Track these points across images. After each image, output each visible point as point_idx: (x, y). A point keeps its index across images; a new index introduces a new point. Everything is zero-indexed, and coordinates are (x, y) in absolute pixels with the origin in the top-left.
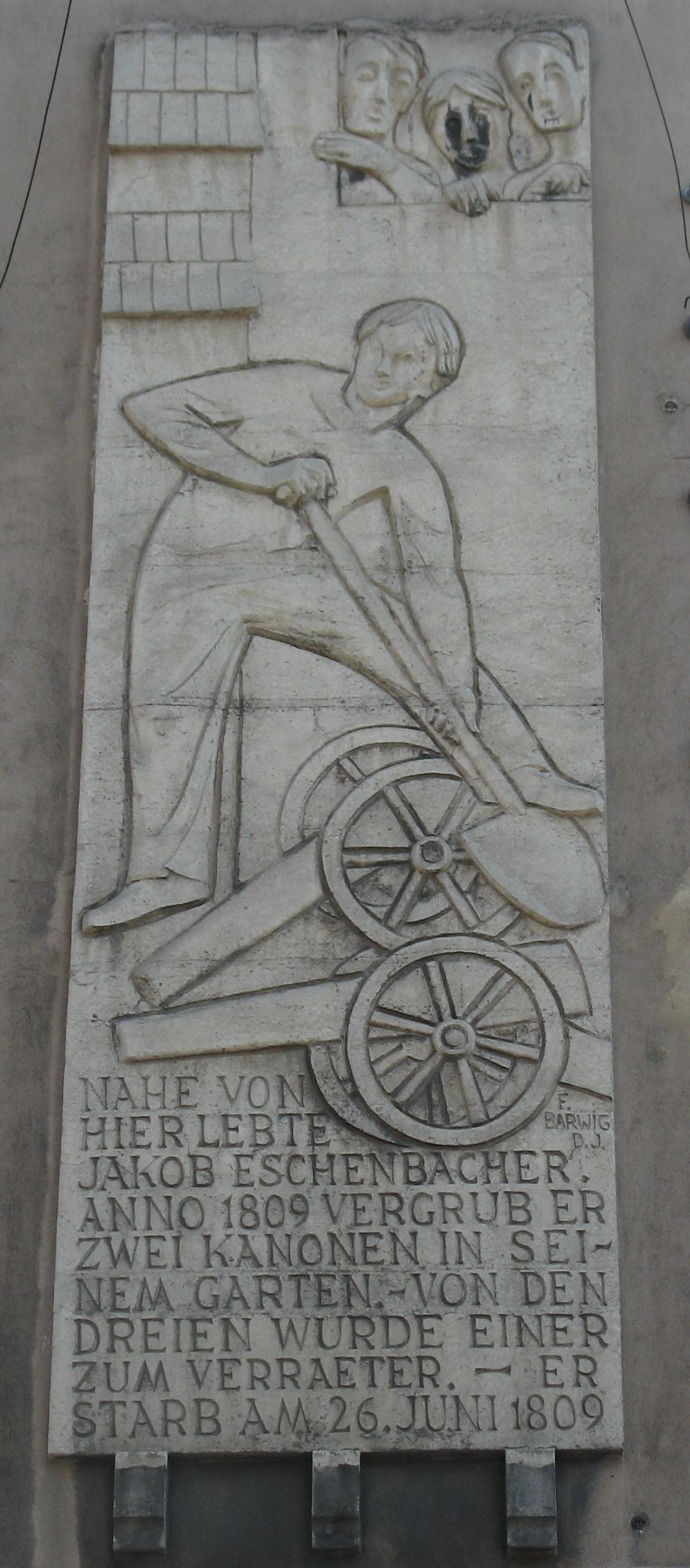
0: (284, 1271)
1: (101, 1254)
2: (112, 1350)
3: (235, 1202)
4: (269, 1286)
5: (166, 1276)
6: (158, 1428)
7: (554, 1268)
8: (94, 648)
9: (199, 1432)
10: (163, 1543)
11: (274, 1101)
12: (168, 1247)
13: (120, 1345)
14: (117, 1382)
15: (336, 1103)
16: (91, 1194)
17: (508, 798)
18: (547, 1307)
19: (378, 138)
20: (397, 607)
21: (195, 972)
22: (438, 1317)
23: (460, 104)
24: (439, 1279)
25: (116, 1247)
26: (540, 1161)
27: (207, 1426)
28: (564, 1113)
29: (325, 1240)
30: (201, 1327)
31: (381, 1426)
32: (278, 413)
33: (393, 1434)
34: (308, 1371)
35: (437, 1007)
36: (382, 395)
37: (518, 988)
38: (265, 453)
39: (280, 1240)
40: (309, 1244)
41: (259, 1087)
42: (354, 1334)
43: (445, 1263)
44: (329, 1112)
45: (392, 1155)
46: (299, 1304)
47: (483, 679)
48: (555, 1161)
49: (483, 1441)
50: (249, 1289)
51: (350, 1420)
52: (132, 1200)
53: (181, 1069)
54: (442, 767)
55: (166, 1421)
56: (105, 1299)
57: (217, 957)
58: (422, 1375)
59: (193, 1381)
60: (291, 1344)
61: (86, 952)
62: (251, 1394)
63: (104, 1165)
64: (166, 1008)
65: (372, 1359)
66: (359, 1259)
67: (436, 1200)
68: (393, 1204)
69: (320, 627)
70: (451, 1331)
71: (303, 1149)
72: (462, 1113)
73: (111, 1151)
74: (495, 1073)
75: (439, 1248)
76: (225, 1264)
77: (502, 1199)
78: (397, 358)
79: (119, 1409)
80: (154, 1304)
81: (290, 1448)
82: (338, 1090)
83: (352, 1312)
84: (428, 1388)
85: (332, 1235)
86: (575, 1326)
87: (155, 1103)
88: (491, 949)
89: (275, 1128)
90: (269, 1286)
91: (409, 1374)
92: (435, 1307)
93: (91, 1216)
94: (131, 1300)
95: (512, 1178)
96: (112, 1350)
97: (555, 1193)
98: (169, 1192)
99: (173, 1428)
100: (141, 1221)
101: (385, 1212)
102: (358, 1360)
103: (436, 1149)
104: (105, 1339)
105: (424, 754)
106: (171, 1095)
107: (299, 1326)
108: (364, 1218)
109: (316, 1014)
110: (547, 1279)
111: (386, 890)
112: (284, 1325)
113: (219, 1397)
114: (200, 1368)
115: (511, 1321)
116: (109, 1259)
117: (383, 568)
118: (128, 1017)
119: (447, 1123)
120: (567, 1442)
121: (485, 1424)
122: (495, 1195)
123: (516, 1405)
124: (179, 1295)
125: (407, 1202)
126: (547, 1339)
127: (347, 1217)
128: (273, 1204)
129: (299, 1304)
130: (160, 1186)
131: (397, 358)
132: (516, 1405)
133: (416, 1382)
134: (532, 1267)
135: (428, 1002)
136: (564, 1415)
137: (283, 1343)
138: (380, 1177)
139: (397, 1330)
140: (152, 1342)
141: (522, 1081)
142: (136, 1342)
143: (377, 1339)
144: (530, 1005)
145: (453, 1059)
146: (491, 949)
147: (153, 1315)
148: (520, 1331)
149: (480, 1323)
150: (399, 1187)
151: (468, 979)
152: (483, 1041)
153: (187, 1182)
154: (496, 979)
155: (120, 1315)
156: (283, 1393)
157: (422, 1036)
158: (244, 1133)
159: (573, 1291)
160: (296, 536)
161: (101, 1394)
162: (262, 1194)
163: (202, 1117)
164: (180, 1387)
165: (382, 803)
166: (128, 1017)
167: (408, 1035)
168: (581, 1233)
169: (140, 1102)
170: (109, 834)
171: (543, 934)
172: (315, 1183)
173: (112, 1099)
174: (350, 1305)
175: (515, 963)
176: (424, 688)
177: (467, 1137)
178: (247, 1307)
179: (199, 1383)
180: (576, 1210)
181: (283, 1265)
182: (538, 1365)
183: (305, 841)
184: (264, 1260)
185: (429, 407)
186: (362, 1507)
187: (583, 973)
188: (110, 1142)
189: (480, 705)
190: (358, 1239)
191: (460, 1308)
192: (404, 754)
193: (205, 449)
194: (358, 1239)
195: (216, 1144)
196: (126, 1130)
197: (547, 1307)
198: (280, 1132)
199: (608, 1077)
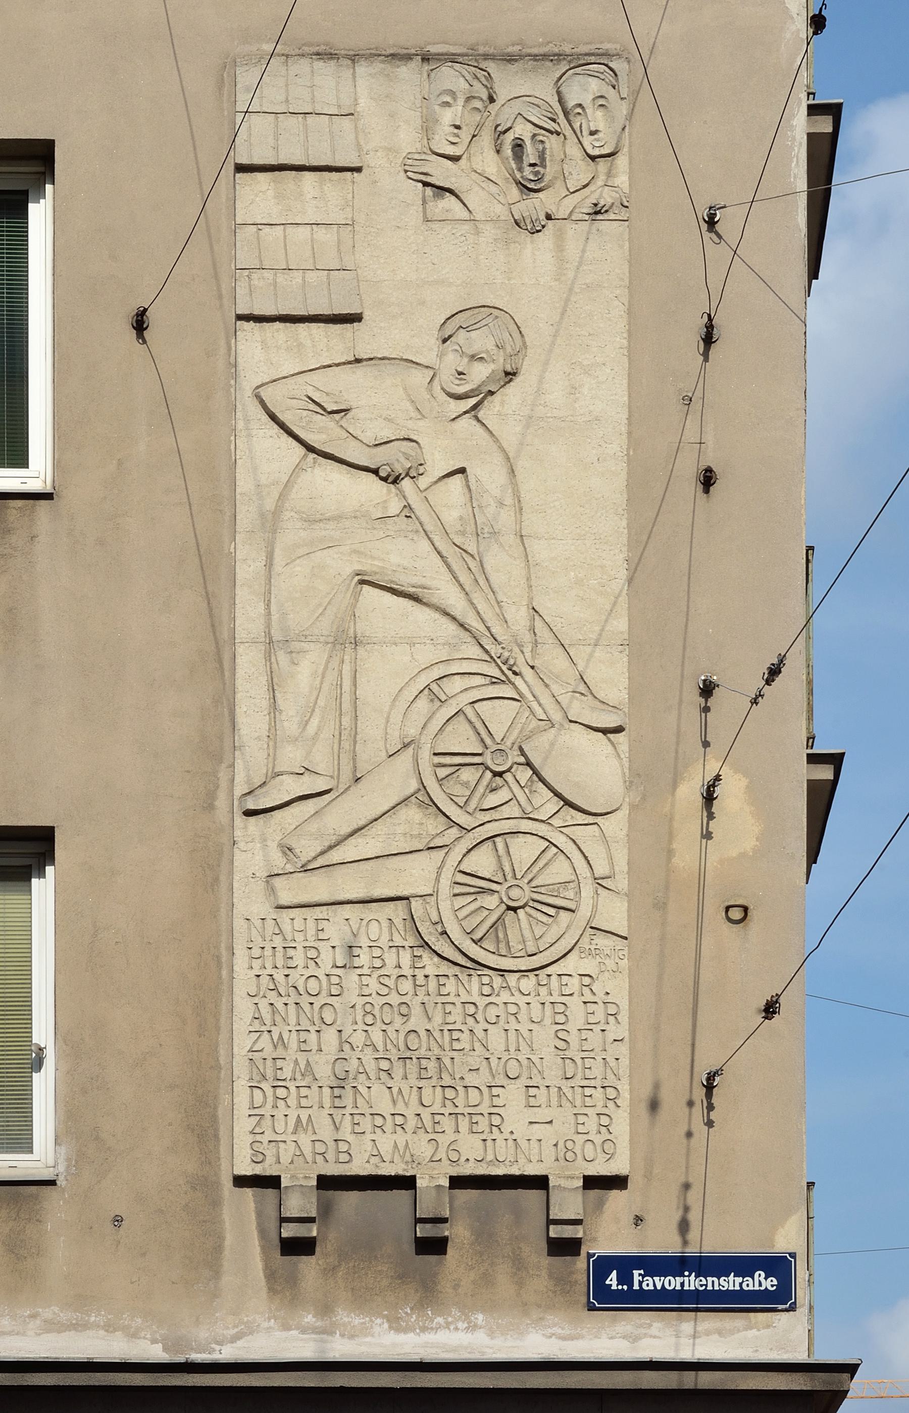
0: (394, 1055)
1: (265, 1042)
2: (275, 1106)
4: (385, 1065)
5: (314, 1058)
6: (309, 1159)
8: (241, 593)
9: (337, 1162)
12: (313, 1036)
13: (281, 1103)
16: (256, 1000)
17: (557, 716)
18: (578, 1081)
19: (455, 159)
20: (472, 564)
21: (327, 844)
23: (523, 130)
24: (503, 1060)
25: (276, 1037)
26: (576, 981)
27: (344, 1157)
29: (423, 1033)
31: (463, 1159)
32: (378, 407)
33: (472, 1163)
34: (412, 1122)
36: (461, 390)
37: (562, 857)
38: (369, 437)
39: (392, 1034)
40: (413, 1035)
47: (538, 623)
48: (587, 981)
49: (532, 1170)
50: (371, 1066)
53: (319, 912)
54: (509, 692)
56: (269, 1073)
57: (342, 833)
59: (332, 1127)
60: (400, 1104)
61: (245, 828)
62: (373, 1137)
63: (265, 980)
64: (305, 869)
66: (447, 1047)
67: (502, 1006)
68: (471, 1009)
69: (415, 580)
70: (513, 1095)
73: (269, 971)
74: (545, 919)
75: (503, 1041)
77: (548, 1006)
78: (473, 358)
79: (282, 1145)
81: (401, 1173)
82: (432, 929)
86: (598, 1094)
87: (299, 937)
88: (542, 829)
89: (386, 956)
90: (385, 1065)
93: (256, 1016)
94: (287, 1073)
95: (556, 993)
96: (275, 1106)
97: (585, 1003)
98: (312, 1000)
99: (319, 1159)
100: (292, 1020)
102: (447, 1115)
103: (502, 972)
104: (270, 1099)
105: (495, 681)
106: (311, 932)
107: (406, 1092)
108: (450, 1019)
109: (415, 875)
110: (579, 1062)
111: (466, 784)
113: (350, 1138)
115: (554, 1090)
116: (271, 1045)
117: (463, 533)
121: (535, 1158)
125: (481, 1008)
126: (578, 1103)
127: (438, 1019)
130: (305, 996)
131: (473, 358)
133: (487, 1130)
134: (568, 1054)
136: (590, 1155)
137: (394, 1102)
138: (462, 991)
140: (304, 1102)
141: (564, 925)
143: (460, 1101)
144: (571, 871)
145: (515, 909)
146: (542, 829)
149: (532, 1091)
150: (475, 998)
151: (524, 851)
152: (535, 896)
155: (280, 1083)
156: (395, 1136)
159: (597, 1070)
160: (395, 506)
161: (269, 1135)
162: (378, 1001)
163: (333, 947)
164: (326, 1132)
165: (461, 718)
167: (483, 891)
169: (289, 938)
170: (259, 738)
171: (580, 818)
175: (560, 840)
176: (493, 631)
179: (337, 1129)
180: (600, 1016)
181: (394, 1051)
182: (572, 1119)
183: (406, 746)
184: (380, 1047)
185: (497, 398)
187: (609, 845)
188: (269, 965)
189: (536, 643)
190: (446, 1033)
191: (517, 1081)
192: (479, 680)
193: (320, 431)
194: (446, 1033)
195: (344, 967)
197: (578, 1081)
198: (390, 958)
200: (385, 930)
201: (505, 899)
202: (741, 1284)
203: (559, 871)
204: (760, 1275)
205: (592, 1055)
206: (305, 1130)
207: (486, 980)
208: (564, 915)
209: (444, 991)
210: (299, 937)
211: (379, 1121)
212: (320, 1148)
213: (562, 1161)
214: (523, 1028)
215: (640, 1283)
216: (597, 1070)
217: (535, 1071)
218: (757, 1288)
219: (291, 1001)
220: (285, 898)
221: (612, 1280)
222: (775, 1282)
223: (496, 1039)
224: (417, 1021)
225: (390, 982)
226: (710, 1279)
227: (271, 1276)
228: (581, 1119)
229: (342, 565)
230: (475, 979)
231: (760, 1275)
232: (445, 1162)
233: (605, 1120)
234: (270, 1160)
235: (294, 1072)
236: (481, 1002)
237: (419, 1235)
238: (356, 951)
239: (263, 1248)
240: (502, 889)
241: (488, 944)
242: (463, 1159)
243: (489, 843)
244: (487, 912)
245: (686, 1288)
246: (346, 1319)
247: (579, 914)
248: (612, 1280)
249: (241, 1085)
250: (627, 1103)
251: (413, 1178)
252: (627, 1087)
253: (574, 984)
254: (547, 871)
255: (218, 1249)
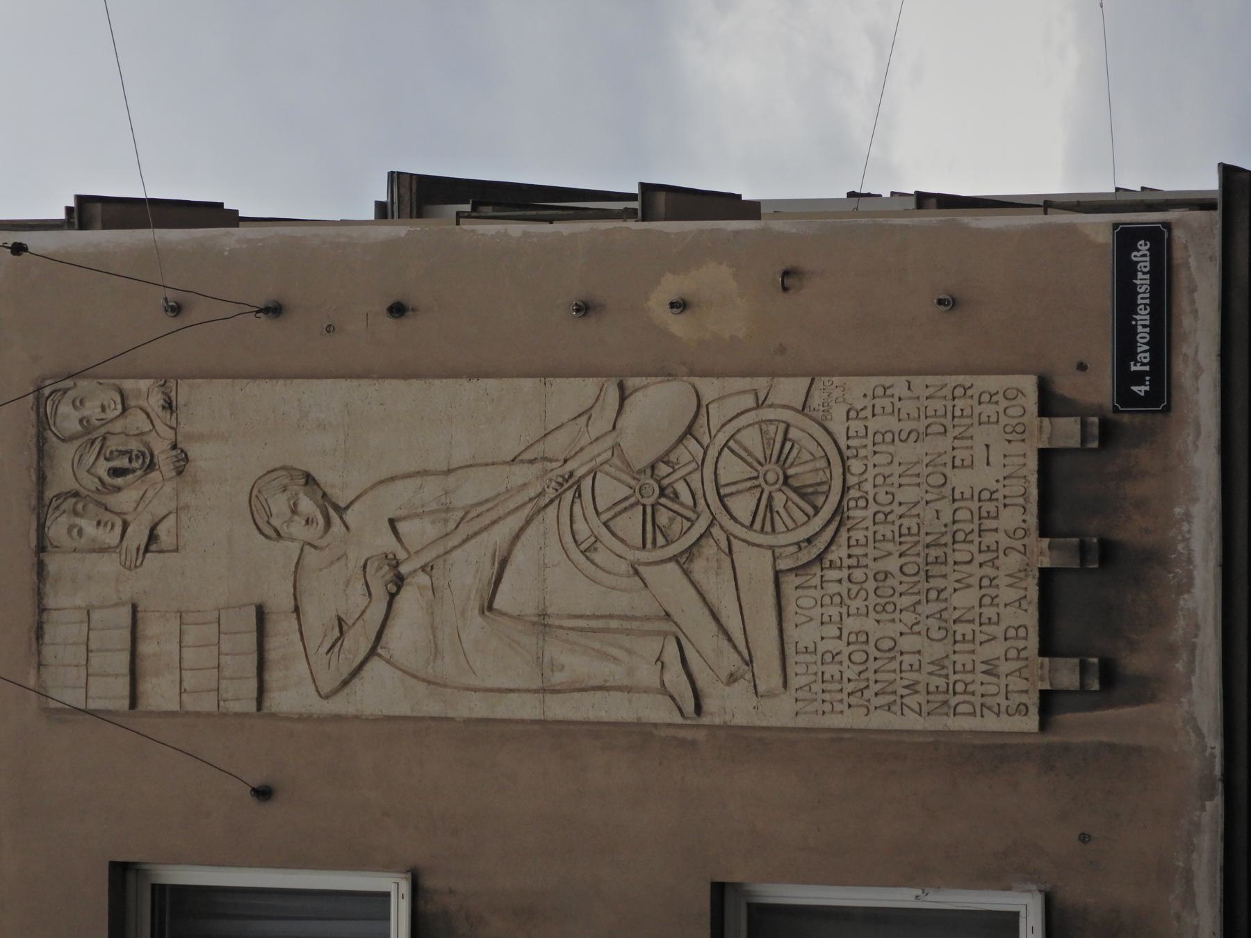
2: (973, 693)
3: (878, 617)
4: (933, 595)
5: (926, 659)
6: (1023, 663)
7: (923, 417)
8: (501, 713)
9: (1026, 638)
10: (1095, 660)
11: (812, 592)
12: (907, 659)
13: (970, 688)
14: (992, 689)
15: (814, 552)
16: (872, 708)
17: (609, 441)
18: (948, 421)
19: (125, 525)
20: (473, 514)
21: (726, 643)
22: (953, 489)
23: (102, 468)
24: (929, 489)
25: (907, 691)
26: (852, 424)
27: (1022, 632)
28: (821, 408)
29: (904, 560)
30: (959, 637)
31: (1023, 525)
32: (336, 593)
34: (988, 570)
35: (751, 488)
36: (321, 521)
37: (738, 437)
38: (363, 601)
39: (904, 588)
40: (906, 569)
41: (802, 602)
42: (964, 541)
43: (919, 485)
44: (820, 558)
45: (848, 518)
46: (945, 576)
47: (526, 456)
48: (853, 414)
49: (1033, 463)
50: (934, 607)
51: (1018, 544)
52: (876, 682)
53: (790, 650)
54: (586, 485)
55: (1018, 658)
56: (941, 698)
58: (990, 499)
61: (711, 714)
62: (1001, 606)
63: (853, 700)
64: (749, 662)
65: (980, 531)
66: (915, 539)
67: (877, 489)
68: (880, 517)
69: (488, 564)
70: (961, 480)
71: (844, 574)
72: (821, 473)
73: (845, 696)
74: (795, 451)
75: (910, 488)
76: (918, 623)
77: (877, 448)
78: (294, 511)
79: (1010, 688)
80: (943, 667)
81: (1036, 581)
82: (805, 551)
83: (950, 542)
84: (999, 495)
85: (901, 555)
86: (960, 403)
87: (813, 669)
88: (713, 453)
89: (830, 592)
90: (933, 595)
91: (989, 507)
92: (947, 491)
94: (941, 682)
95: (865, 441)
96: (973, 693)
97: (874, 415)
98: (871, 658)
99: (1023, 654)
100: (892, 676)
101: (885, 522)
103: (845, 489)
104: (967, 698)
105: (578, 494)
106: (808, 658)
107: (958, 576)
109: (756, 565)
110: (930, 420)
111: (672, 520)
112: (957, 585)
113: (1003, 626)
114: (985, 638)
115: (957, 443)
117: (446, 521)
118: (755, 686)
119: (828, 482)
120: (1033, 407)
121: (1021, 460)
122: (875, 453)
123: (1009, 441)
124: (938, 650)
125: (879, 508)
126: (968, 421)
127: (889, 546)
128: (878, 592)
129: (945, 576)
130: (868, 664)
131: (294, 511)
132: (1009, 441)
133: (995, 503)
134: (922, 430)
135: (747, 494)
136: (1019, 411)
137: (969, 586)
139: (961, 515)
141: (801, 434)
142: (969, 678)
143: (967, 527)
145: (786, 478)
146: (713, 453)
147: (951, 668)
148: (963, 438)
149: (958, 462)
150: (870, 513)
151: (732, 469)
153: (865, 647)
154: (732, 451)
157: (770, 498)
158: (834, 611)
159: (938, 405)
160: (423, 579)
161: (1001, 699)
162: (873, 599)
164: (997, 649)
165: (611, 524)
166: (755, 686)
167: (770, 506)
168: (900, 399)
169: (812, 678)
170: (630, 701)
171: (702, 420)
172: (866, 566)
173: (808, 696)
174: (945, 545)
175: (722, 438)
176: (533, 495)
177: (837, 470)
178: (946, 609)
179: (994, 638)
180: (886, 402)
181: (919, 586)
182: (984, 427)
183: (636, 572)
184: (916, 598)
185: (329, 491)
186: (1073, 536)
187: (727, 397)
188: (839, 696)
189: (544, 459)
190: (902, 539)
191: (948, 475)
192: (577, 508)
193: (357, 642)
194: (902, 539)
195: (840, 629)
196: (828, 686)
197: (948, 421)
198: (833, 588)
199: (799, 380)
200: (806, 592)
201: (777, 486)
202: (1144, 273)
203: (751, 439)
204: (1135, 256)
205: (922, 409)
206: (996, 666)
207: (852, 504)
208: (793, 433)
209: (863, 541)
210: (813, 669)
211: (987, 600)
212: (1013, 654)
213: (1024, 436)
214: (897, 470)
215: (1143, 364)
216: (938, 405)
217: (939, 461)
218: (1147, 259)
219: (873, 677)
220: (777, 680)
221: (1141, 390)
222: (1142, 242)
223: (909, 494)
224: (893, 564)
225: (855, 588)
226: (1139, 301)
227: (1137, 700)
228: (984, 419)
229: (476, 624)
230: (851, 513)
231: (1135, 256)
232: (1026, 541)
233: (986, 397)
234: (1024, 698)
235: (940, 676)
236: (873, 508)
237: (1096, 566)
238: (826, 619)
239: (1110, 707)
240: (767, 489)
241: (819, 500)
242: (1023, 525)
243: (728, 501)
244: (790, 503)
245: (1147, 323)
246: (1180, 632)
247: (790, 421)
248: (1141, 390)
249: (954, 724)
250: (968, 377)
251: (1042, 570)
252: (954, 377)
253: (856, 426)
254: (750, 449)
255: (1112, 747)
